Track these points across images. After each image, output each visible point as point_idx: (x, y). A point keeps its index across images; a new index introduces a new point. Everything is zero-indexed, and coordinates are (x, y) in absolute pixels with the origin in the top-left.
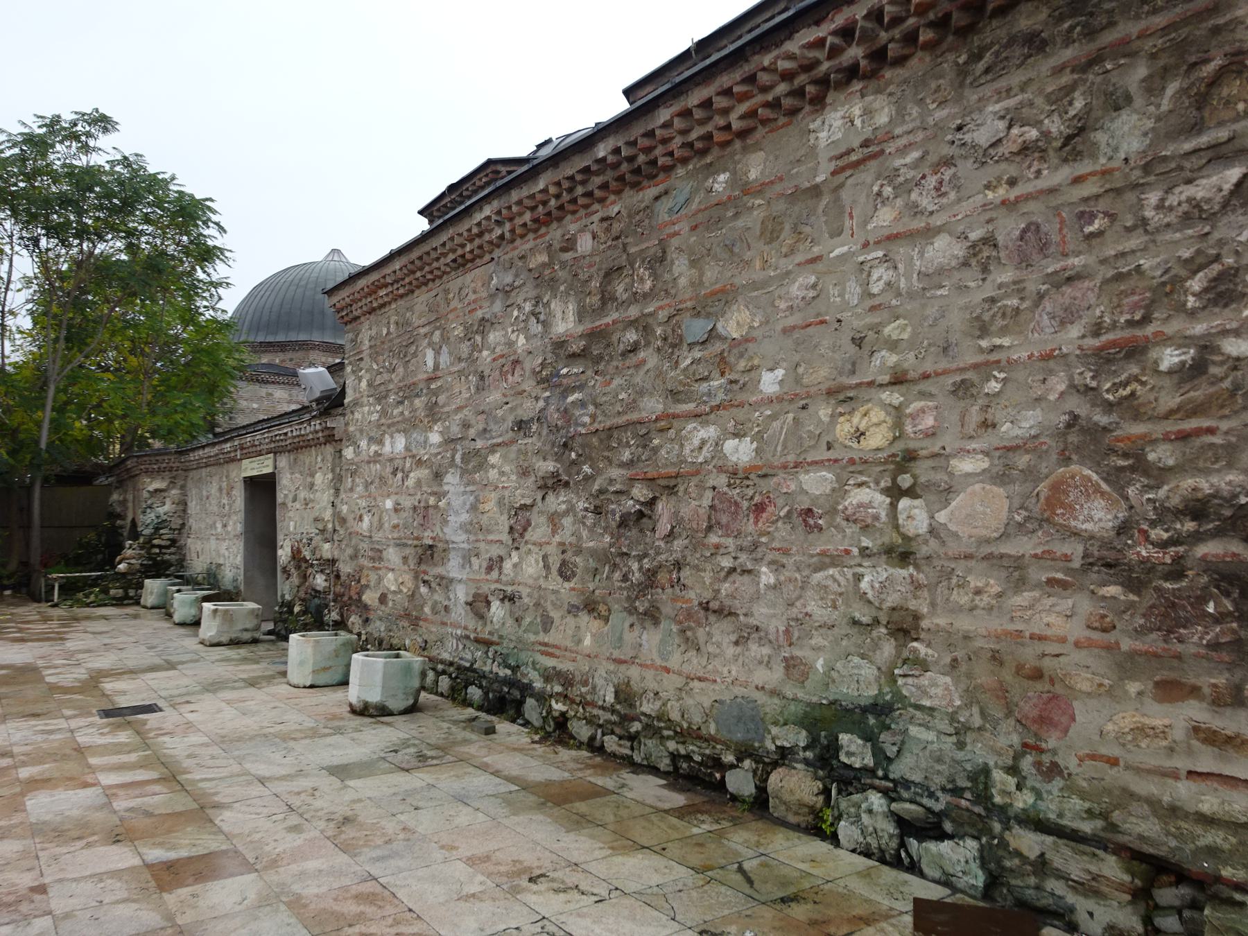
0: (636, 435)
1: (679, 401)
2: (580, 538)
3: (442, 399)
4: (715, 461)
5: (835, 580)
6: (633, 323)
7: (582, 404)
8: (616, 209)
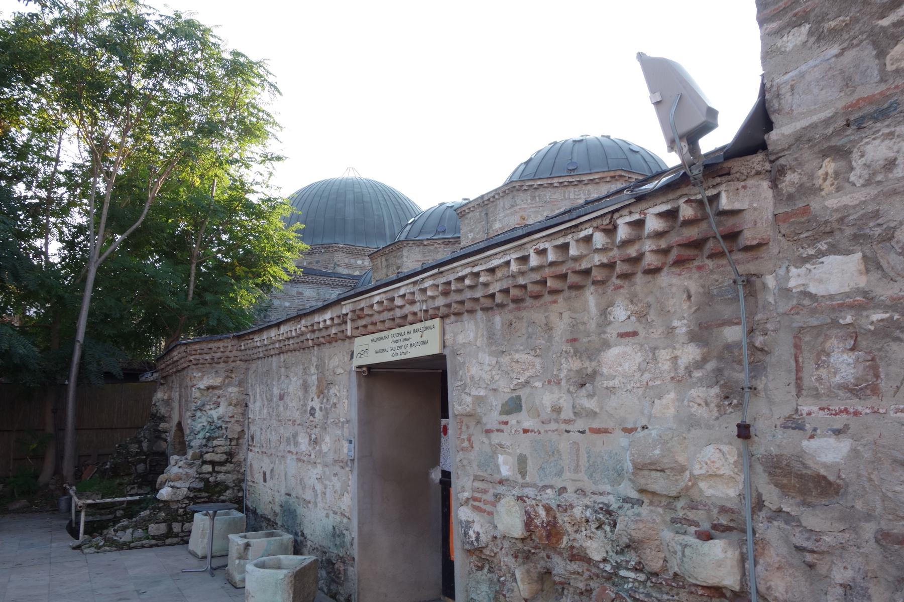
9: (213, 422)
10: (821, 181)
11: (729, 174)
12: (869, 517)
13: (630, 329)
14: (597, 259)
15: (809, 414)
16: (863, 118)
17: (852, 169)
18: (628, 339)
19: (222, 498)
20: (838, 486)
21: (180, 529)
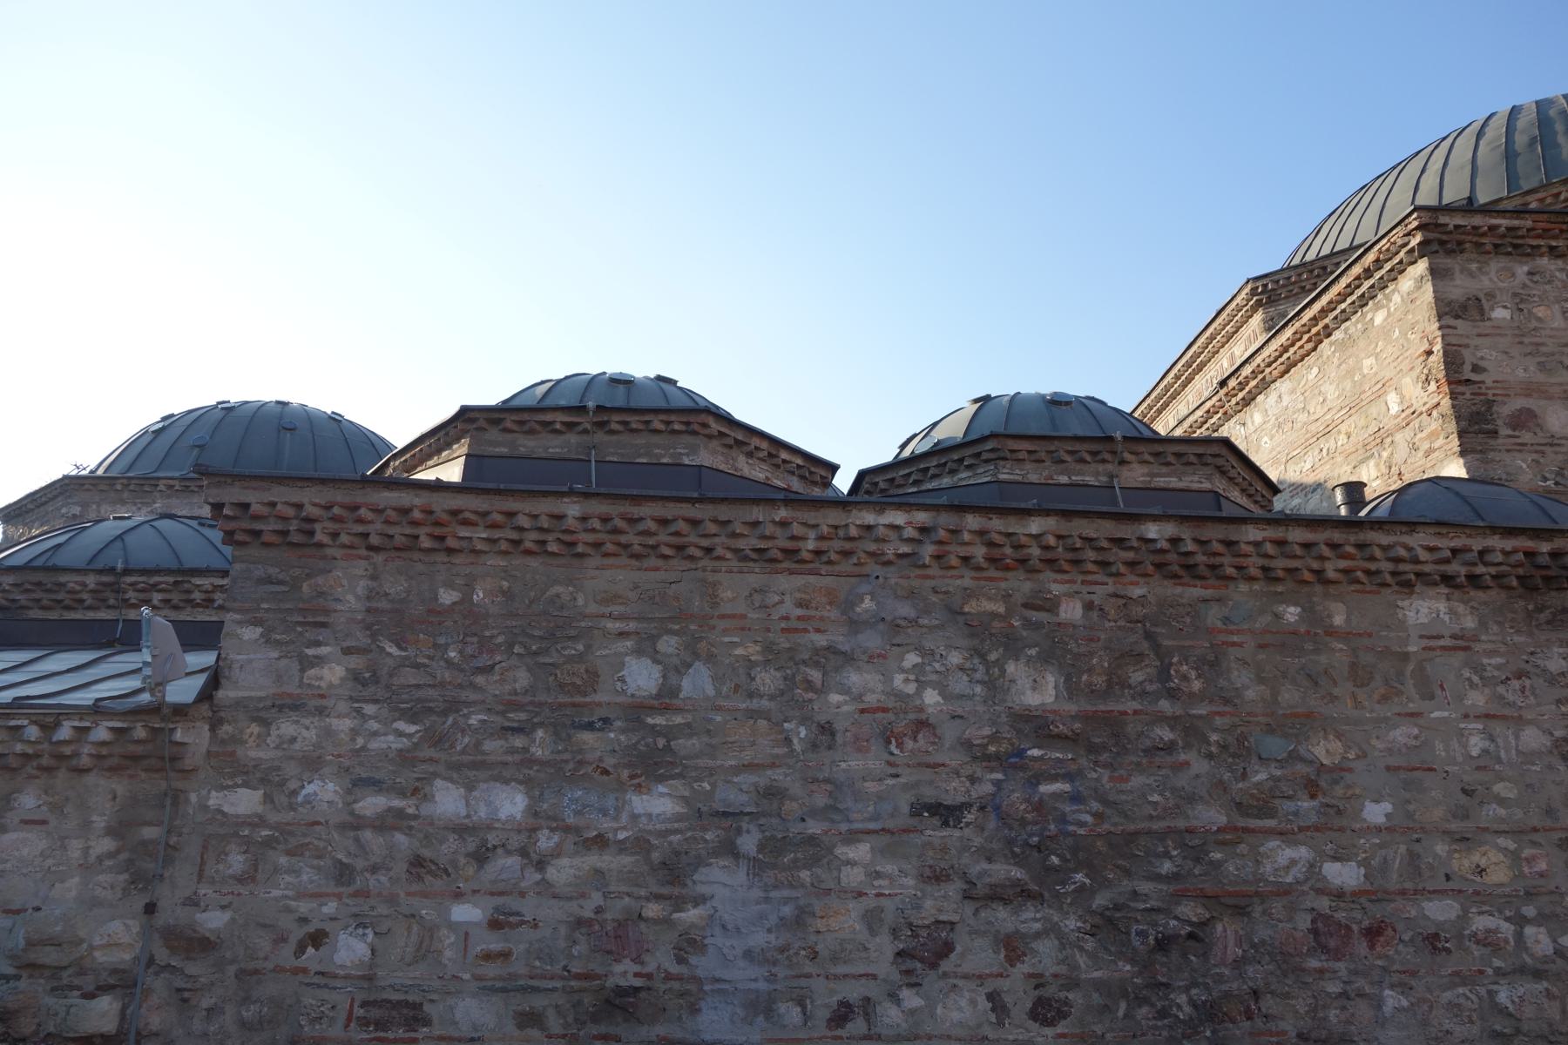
0: (1183, 845)
1: (1248, 815)
2: (1075, 967)
3: (684, 745)
4: (1310, 883)
5: (1468, 998)
6: (1172, 721)
7: (1076, 798)
8: (1137, 592)
10: (247, 737)
11: (186, 715)
12: (233, 961)
13: (36, 817)
14: (19, 748)
15: (205, 895)
16: (284, 705)
17: (269, 735)
18: (33, 826)
20: (216, 944)
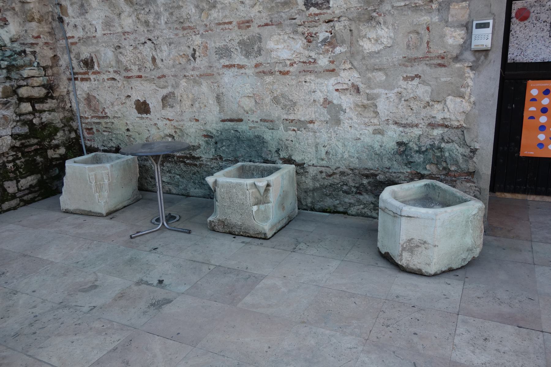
9: (5, 46)
19: (54, 142)
21: (16, 188)
